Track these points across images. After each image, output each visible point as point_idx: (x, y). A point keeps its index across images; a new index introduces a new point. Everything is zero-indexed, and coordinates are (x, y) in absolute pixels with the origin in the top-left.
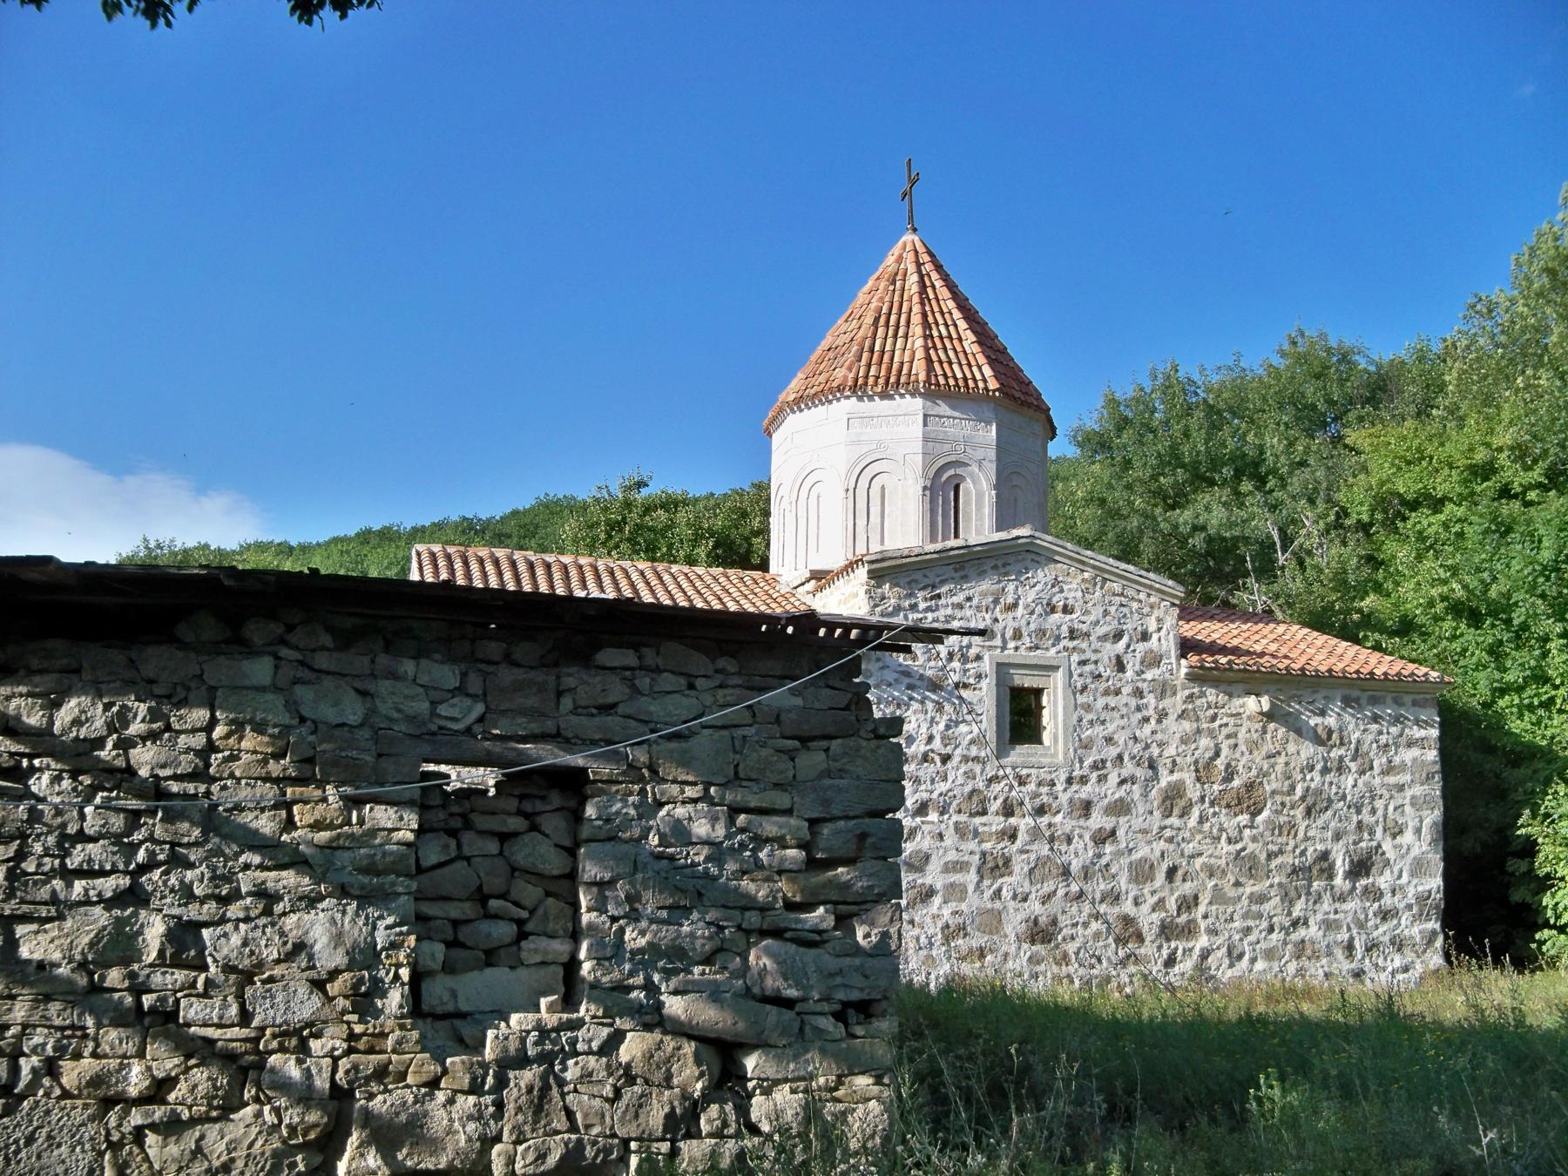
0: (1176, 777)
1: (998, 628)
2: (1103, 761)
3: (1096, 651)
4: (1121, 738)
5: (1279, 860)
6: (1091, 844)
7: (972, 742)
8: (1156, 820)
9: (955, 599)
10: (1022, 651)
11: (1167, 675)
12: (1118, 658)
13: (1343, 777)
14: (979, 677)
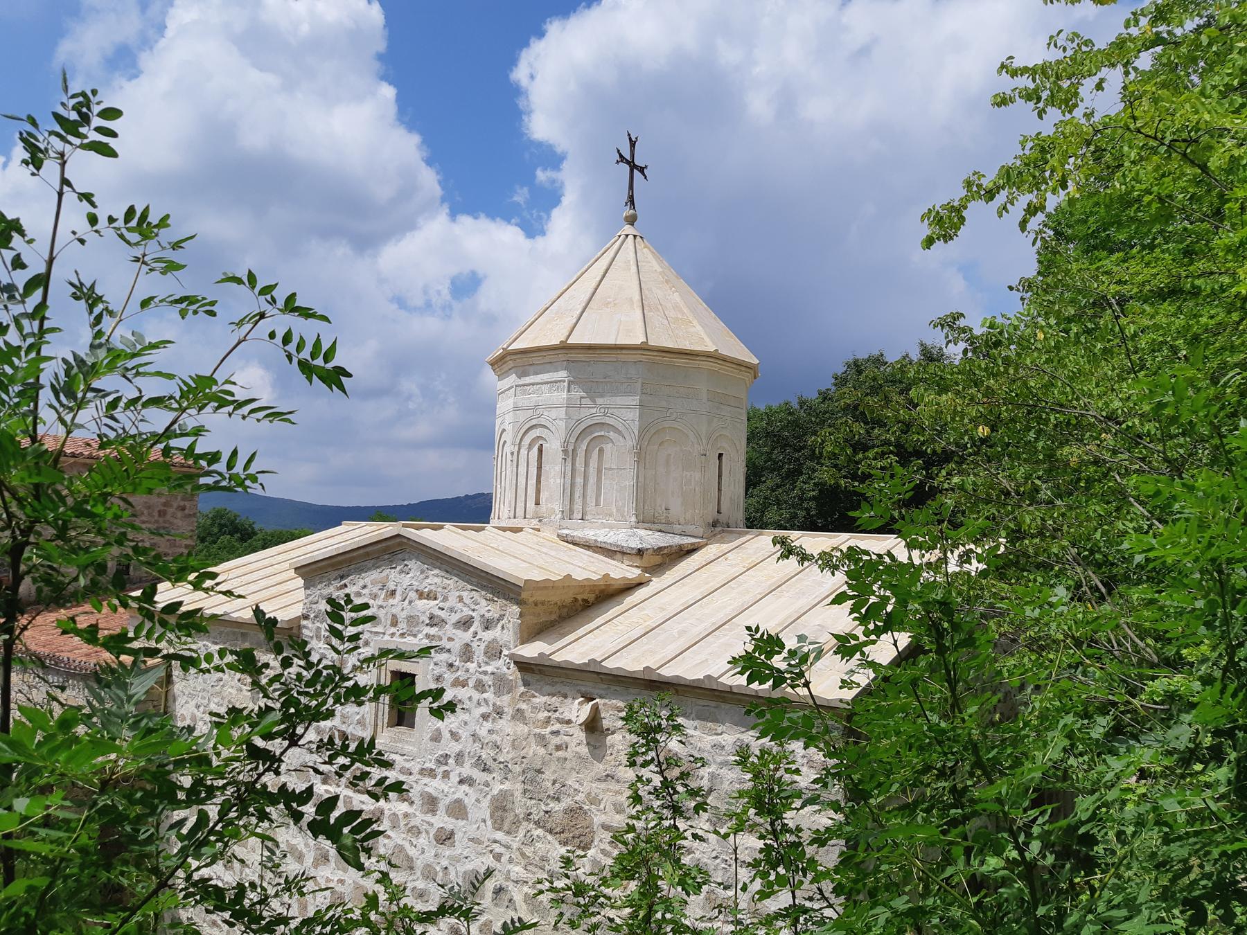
0: (507, 786)
3: (450, 639)
4: (464, 734)
7: (359, 722)
12: (467, 645)
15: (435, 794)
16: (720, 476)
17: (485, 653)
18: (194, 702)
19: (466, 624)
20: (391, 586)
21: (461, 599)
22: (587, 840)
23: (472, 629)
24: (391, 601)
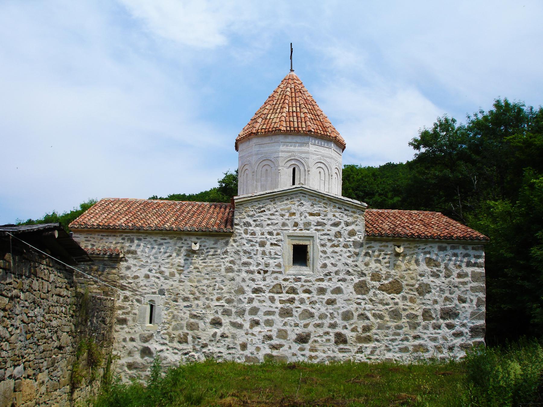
0: (362, 279)
1: (287, 222)
3: (328, 230)
4: (339, 264)
7: (276, 265)
9: (270, 212)
11: (359, 239)
15: (325, 287)
18: (147, 268)
19: (336, 225)
20: (293, 211)
21: (334, 216)
23: (340, 226)
24: (293, 217)
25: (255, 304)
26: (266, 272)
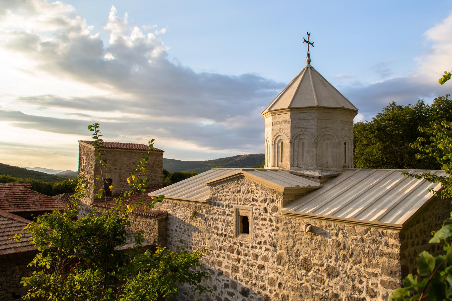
2: (261, 242)
3: (260, 206)
4: (266, 235)
5: (317, 292)
6: (257, 269)
7: (231, 231)
8: (276, 265)
10: (242, 205)
11: (279, 215)
13: (346, 264)
14: (232, 212)
16: (345, 150)
17: (272, 210)
18: (176, 225)
22: (310, 268)
25: (220, 259)
26: (225, 236)
